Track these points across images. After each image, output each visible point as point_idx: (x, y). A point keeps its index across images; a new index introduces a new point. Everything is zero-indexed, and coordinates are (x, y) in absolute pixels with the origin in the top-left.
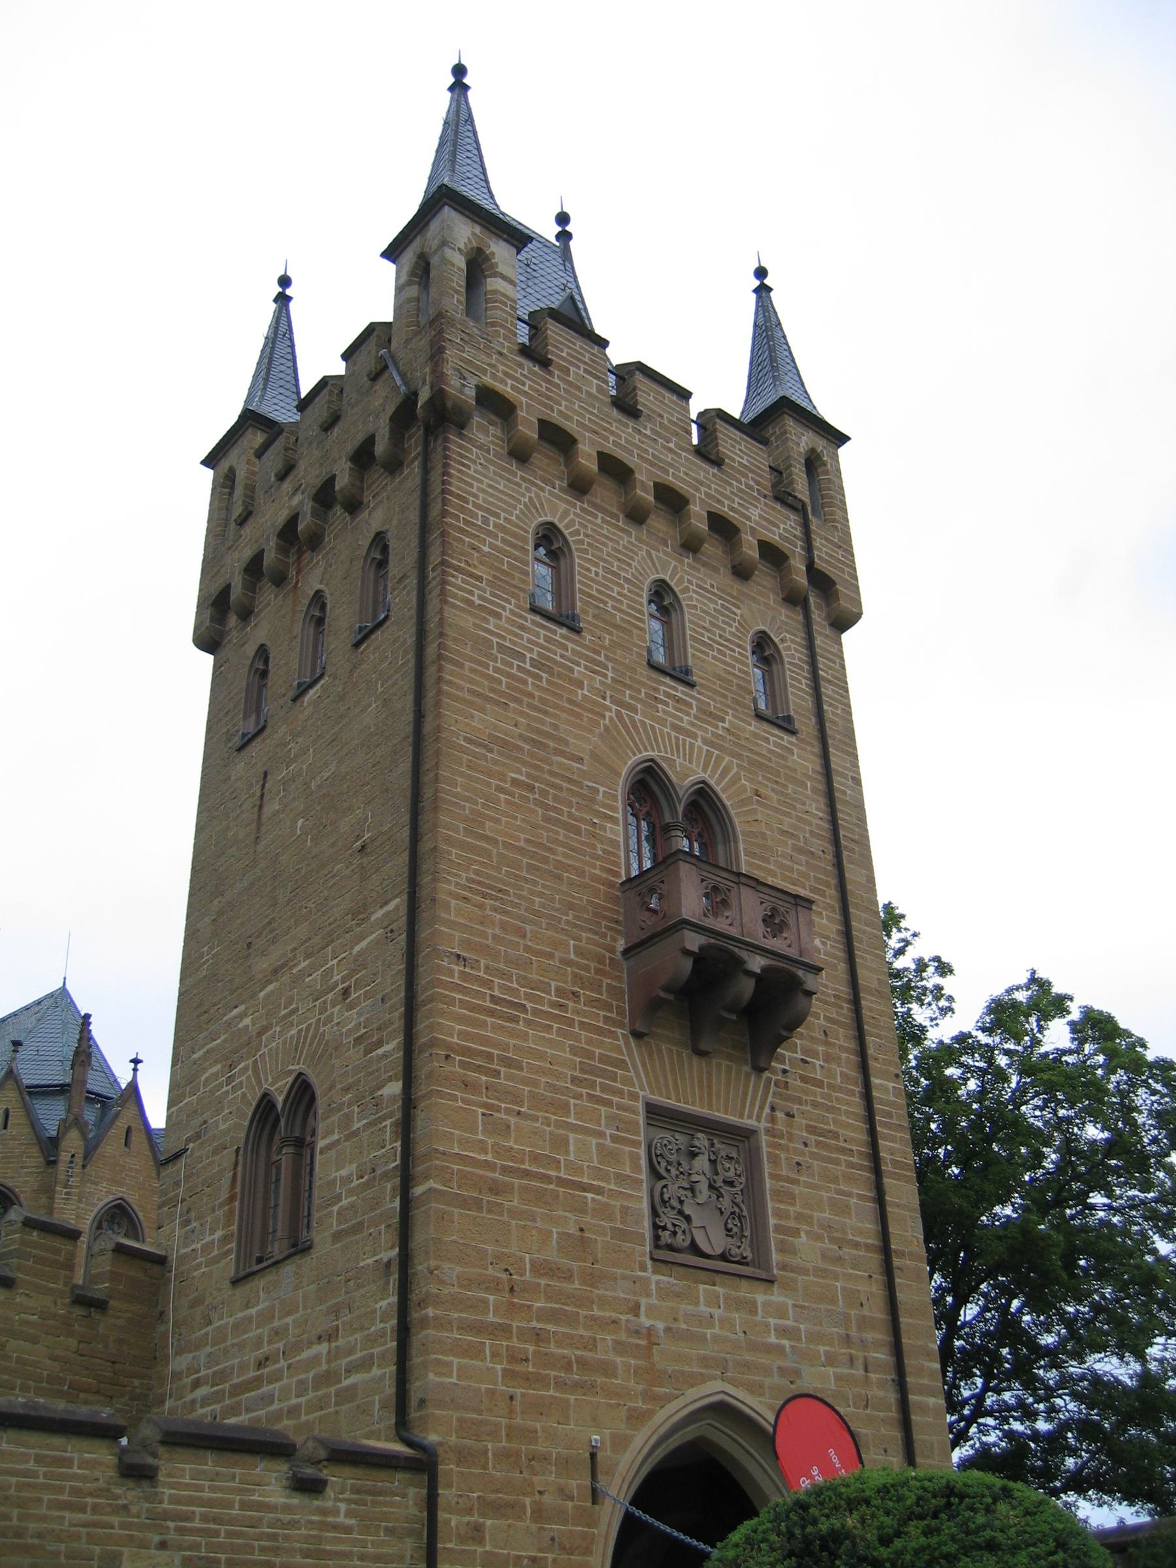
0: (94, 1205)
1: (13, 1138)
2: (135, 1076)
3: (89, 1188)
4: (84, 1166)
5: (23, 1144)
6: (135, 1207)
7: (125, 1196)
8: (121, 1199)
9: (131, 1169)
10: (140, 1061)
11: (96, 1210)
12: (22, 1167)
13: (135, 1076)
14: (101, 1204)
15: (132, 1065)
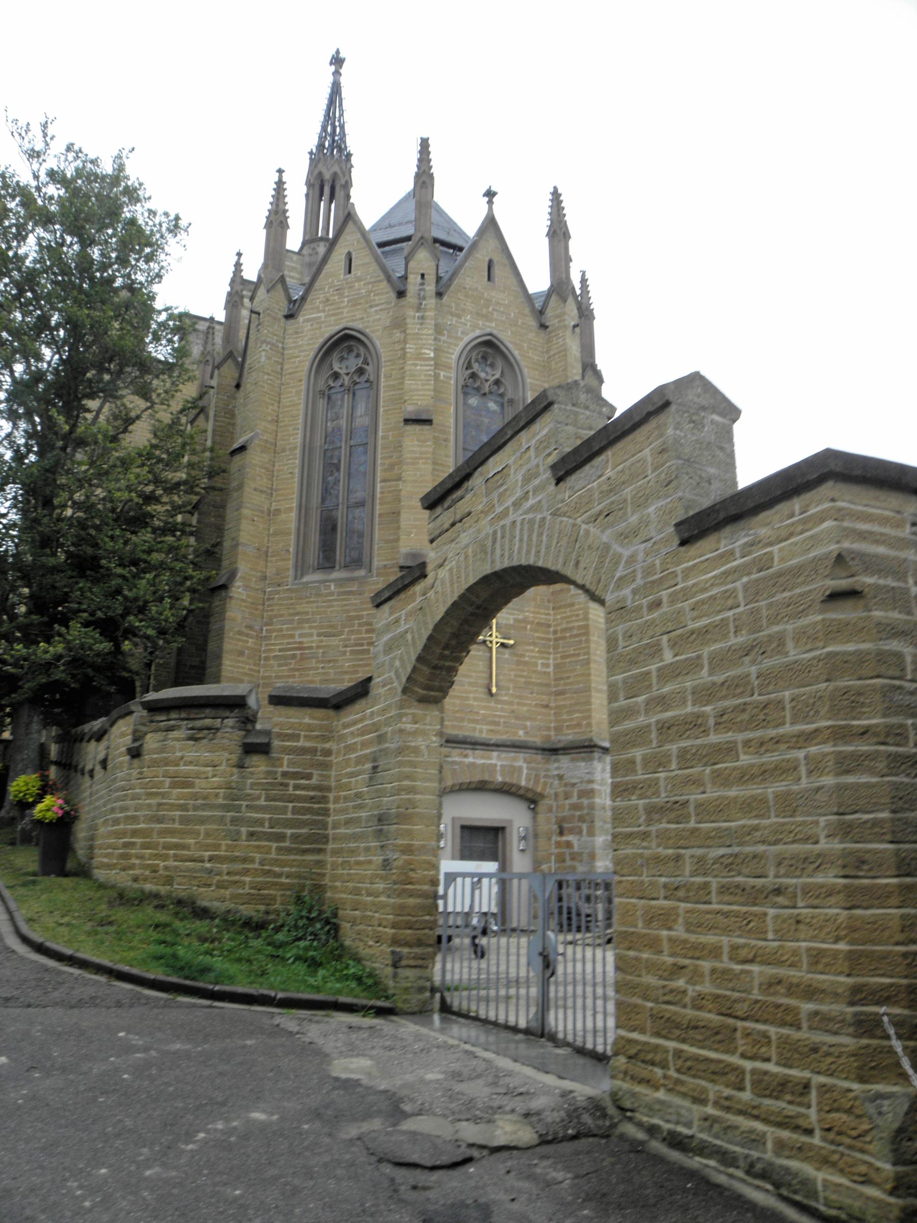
0: (462, 339)
1: (359, 279)
2: (490, 209)
3: (450, 321)
4: (439, 295)
5: (369, 283)
6: (510, 346)
7: (495, 332)
8: (490, 334)
9: (498, 303)
10: (495, 194)
11: (462, 344)
12: (371, 307)
13: (490, 209)
14: (467, 339)
15: (486, 199)
